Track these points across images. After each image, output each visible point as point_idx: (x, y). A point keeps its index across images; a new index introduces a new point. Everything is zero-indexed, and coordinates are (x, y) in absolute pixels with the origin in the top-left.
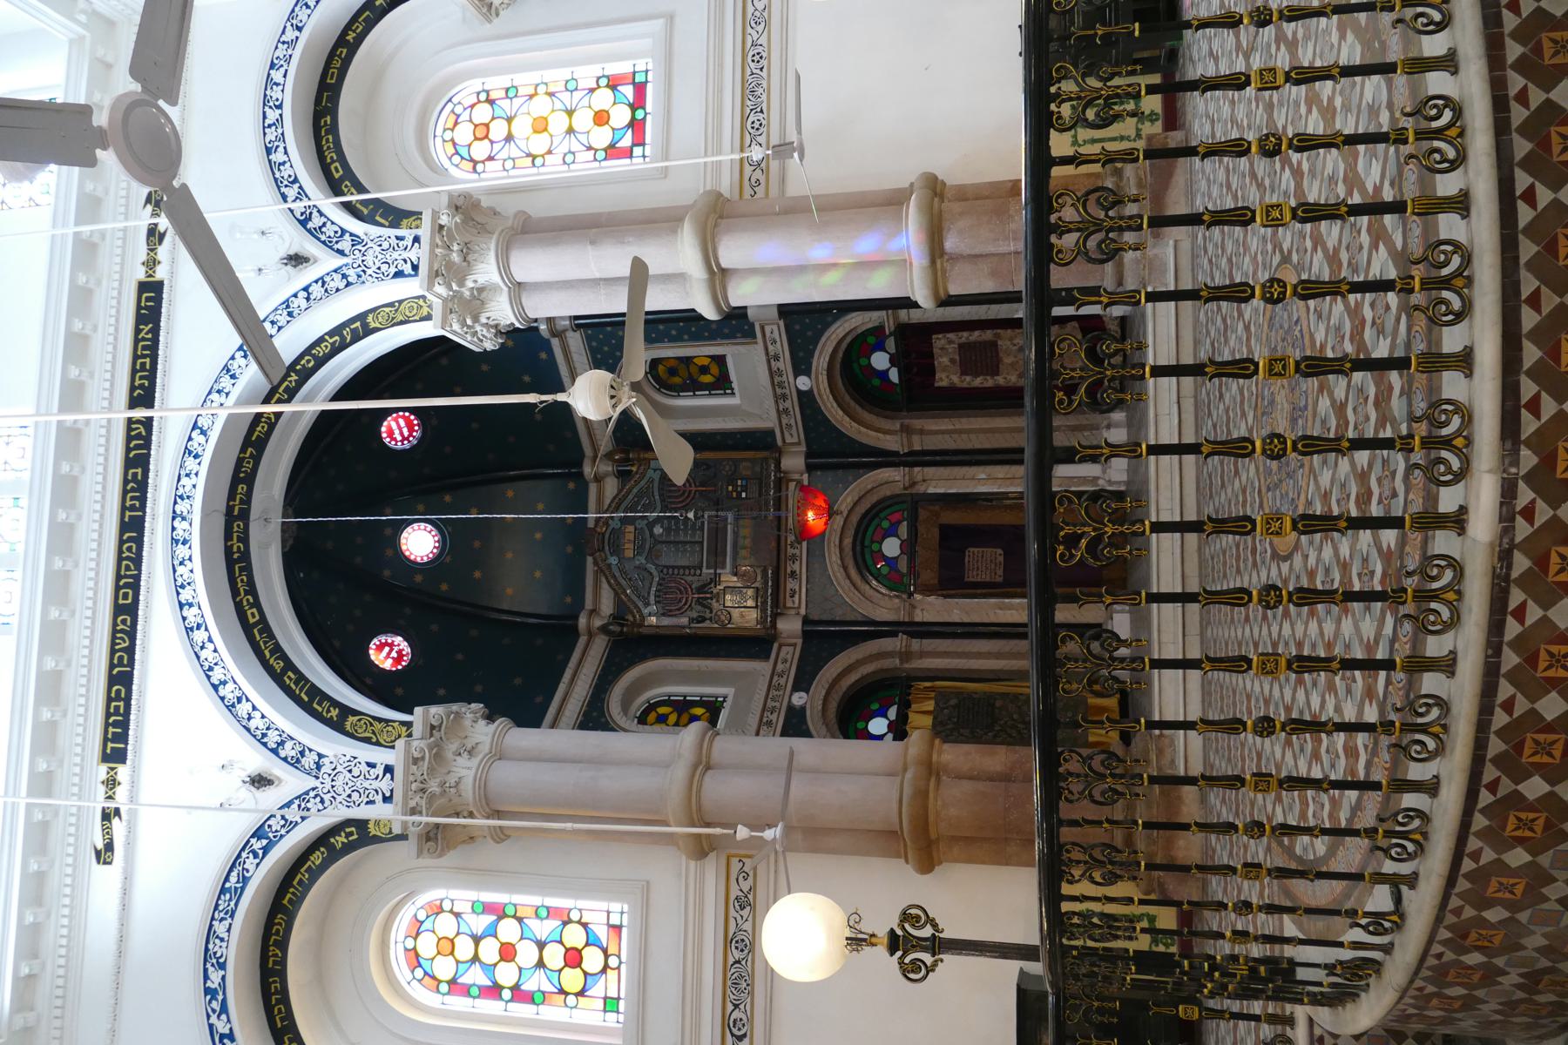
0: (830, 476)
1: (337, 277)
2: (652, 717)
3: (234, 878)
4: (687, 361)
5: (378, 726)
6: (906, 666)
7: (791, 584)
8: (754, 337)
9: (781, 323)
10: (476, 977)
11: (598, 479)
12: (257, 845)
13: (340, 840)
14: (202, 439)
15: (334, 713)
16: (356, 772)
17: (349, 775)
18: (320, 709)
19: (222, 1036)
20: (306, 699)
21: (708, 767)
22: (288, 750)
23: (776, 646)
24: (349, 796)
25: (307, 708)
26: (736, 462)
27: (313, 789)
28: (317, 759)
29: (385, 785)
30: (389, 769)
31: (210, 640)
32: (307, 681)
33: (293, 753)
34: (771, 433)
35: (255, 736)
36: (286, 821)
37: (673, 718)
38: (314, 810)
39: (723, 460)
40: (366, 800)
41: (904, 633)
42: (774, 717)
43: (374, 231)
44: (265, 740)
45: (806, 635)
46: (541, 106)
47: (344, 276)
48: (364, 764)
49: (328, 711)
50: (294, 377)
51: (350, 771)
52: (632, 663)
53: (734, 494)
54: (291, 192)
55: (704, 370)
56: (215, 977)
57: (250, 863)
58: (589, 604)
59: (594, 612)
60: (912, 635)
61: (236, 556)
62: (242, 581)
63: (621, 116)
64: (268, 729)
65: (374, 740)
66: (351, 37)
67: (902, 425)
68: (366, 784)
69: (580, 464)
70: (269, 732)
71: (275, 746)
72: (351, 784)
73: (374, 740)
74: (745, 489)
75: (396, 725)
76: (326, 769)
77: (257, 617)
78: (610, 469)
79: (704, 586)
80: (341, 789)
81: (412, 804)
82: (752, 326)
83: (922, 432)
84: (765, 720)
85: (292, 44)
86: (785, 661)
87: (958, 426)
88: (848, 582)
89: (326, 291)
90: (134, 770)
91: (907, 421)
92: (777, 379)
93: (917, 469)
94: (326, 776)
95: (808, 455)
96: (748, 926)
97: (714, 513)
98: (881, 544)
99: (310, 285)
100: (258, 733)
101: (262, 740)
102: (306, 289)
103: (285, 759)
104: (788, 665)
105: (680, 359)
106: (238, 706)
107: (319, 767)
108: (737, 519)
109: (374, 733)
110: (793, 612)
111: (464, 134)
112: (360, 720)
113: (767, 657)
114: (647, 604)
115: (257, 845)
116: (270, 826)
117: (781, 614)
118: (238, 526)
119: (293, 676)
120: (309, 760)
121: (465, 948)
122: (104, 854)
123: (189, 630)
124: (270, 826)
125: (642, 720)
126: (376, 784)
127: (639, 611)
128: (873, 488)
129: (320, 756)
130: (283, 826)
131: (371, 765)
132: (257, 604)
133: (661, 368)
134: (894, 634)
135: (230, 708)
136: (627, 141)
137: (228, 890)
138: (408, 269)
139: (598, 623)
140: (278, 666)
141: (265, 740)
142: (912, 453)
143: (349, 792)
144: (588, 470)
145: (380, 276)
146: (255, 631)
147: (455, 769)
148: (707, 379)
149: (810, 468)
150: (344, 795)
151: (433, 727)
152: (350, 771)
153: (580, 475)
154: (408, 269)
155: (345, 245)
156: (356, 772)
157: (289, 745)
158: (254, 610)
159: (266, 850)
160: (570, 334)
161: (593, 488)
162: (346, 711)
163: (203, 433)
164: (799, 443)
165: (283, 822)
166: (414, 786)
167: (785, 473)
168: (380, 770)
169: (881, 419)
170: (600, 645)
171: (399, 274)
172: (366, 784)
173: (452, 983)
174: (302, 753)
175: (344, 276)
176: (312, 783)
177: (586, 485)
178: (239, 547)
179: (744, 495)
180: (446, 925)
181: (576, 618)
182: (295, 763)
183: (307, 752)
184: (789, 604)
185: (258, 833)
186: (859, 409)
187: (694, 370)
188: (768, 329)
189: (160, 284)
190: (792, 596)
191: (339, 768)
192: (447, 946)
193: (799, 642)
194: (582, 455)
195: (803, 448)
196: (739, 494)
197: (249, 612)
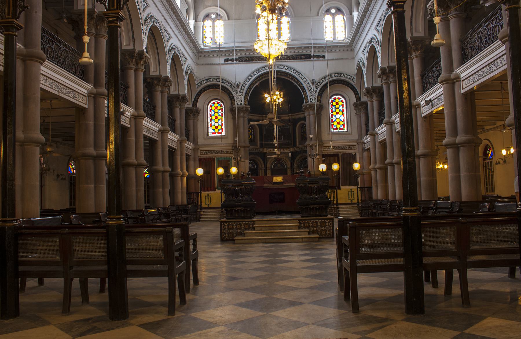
2: (249, 129)
3: (224, 81)
11: (288, 116)
13: (231, 95)
14: (286, 68)
29: (239, 104)
30: (241, 104)
37: (249, 133)
43: (317, 94)
45: (264, 153)
47: (310, 90)
50: (296, 81)
54: (323, 80)
57: (227, 84)
60: (265, 170)
63: (338, 126)
66: (349, 85)
69: (291, 113)
85: (347, 78)
90: (238, 63)
96: (224, 153)
101: (244, 83)
102: (309, 83)
107: (241, 93)
111: (337, 100)
120: (241, 91)
122: (226, 60)
125: (249, 128)
131: (242, 101)
134: (265, 167)
135: (248, 78)
136: (334, 127)
137: (224, 81)
138: (311, 100)
144: (290, 114)
153: (289, 113)
154: (311, 100)
155: (315, 90)
161: (287, 115)
162: (248, 94)
163: (287, 69)
168: (241, 103)
171: (311, 99)
173: (211, 109)
175: (310, 90)
189: (311, 59)
192: (216, 108)
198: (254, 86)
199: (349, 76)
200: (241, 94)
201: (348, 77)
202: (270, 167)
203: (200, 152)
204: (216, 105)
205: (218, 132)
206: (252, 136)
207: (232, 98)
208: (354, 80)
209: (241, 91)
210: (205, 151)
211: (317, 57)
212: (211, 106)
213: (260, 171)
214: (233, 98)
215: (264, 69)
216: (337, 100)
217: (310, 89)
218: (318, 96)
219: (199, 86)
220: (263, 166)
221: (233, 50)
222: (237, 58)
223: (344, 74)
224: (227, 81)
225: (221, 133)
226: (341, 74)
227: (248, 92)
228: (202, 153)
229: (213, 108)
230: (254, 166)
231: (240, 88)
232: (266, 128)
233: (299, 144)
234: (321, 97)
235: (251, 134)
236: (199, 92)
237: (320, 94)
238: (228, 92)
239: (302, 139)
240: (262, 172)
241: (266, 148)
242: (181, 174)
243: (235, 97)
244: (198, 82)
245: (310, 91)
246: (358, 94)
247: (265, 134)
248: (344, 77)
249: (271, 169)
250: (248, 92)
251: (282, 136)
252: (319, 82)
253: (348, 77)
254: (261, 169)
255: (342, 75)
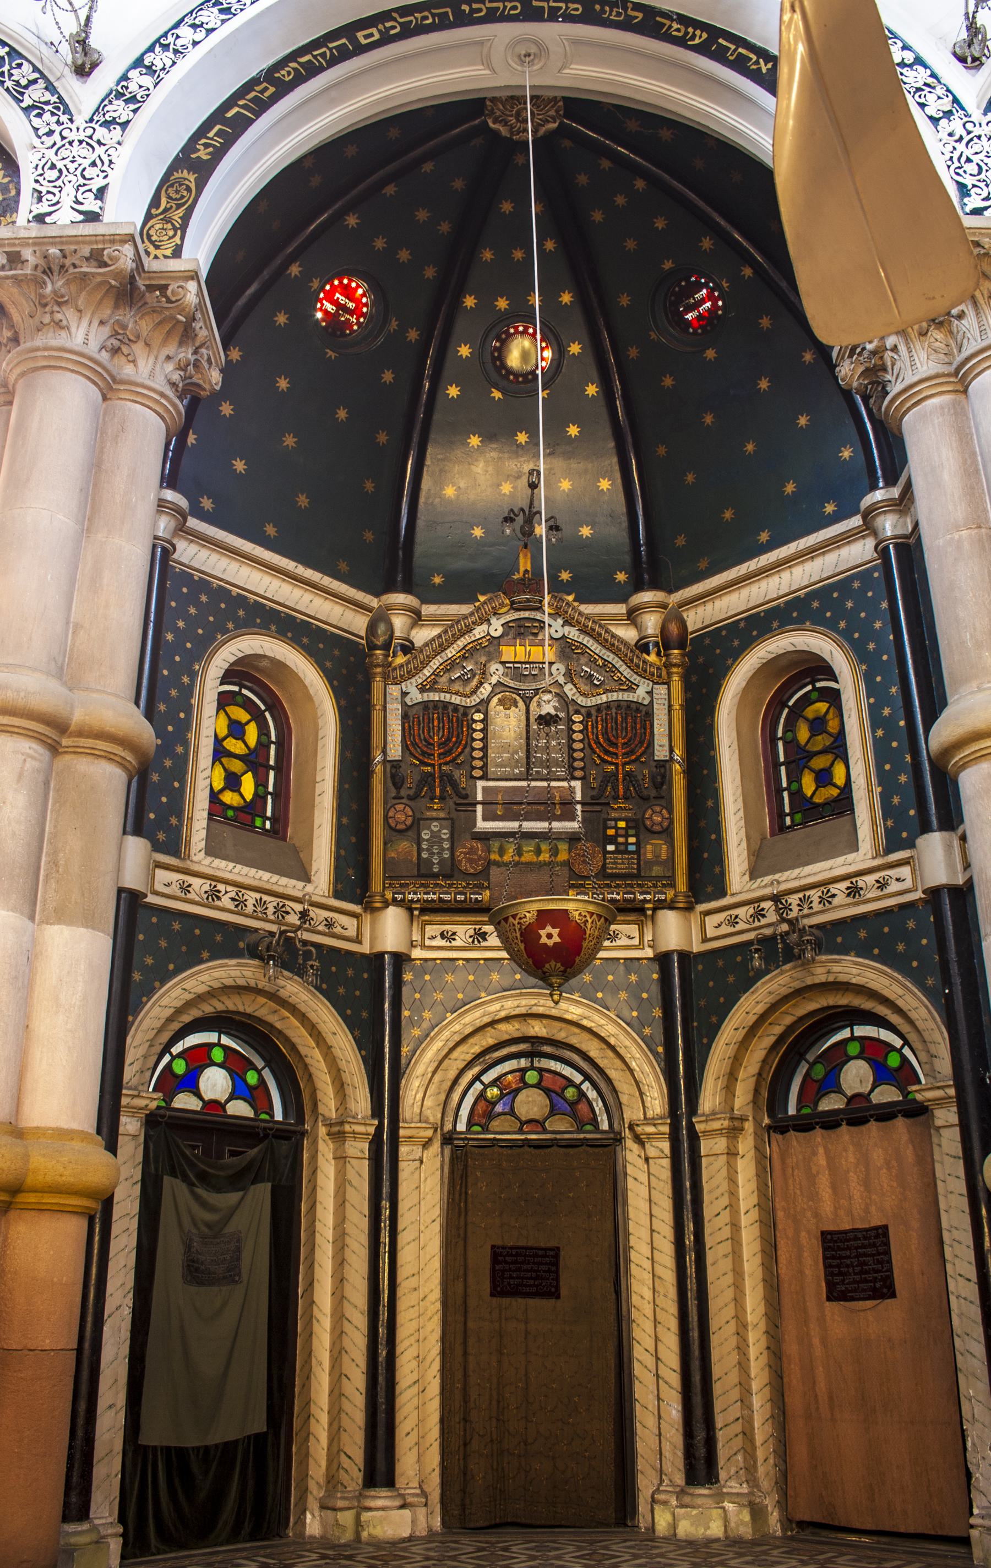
0: (651, 993)
1: (946, 104)
2: (241, 715)
4: (839, 749)
5: (177, 215)
6: (322, 1131)
7: (463, 932)
8: (888, 851)
9: (918, 895)
11: (632, 616)
15: (203, 154)
16: (90, 172)
17: (86, 163)
18: (211, 135)
20: (229, 115)
21: (54, 749)
22: (138, 79)
23: (357, 909)
24: (53, 167)
25: (217, 116)
26: (667, 832)
27: (71, 120)
28: (123, 120)
32: (258, 115)
33: (133, 87)
34: (721, 891)
35: (165, 35)
36: (26, 87)
38: (37, 122)
39: (670, 811)
40: (44, 190)
41: (379, 1129)
42: (226, 902)
44: (158, 49)
48: (103, 183)
49: (206, 146)
51: (94, 164)
52: (330, 676)
53: (611, 832)
55: (824, 778)
58: (427, 610)
59: (417, 618)
60: (376, 1142)
61: (466, 8)
62: (426, 18)
64: (176, 52)
65: (154, 211)
67: (743, 1119)
68: (69, 190)
70: (170, 54)
71: (147, 63)
72: (72, 167)
73: (154, 211)
74: (622, 850)
75: (177, 240)
76: (101, 133)
77: (364, 42)
78: (650, 631)
79: (454, 785)
80: (63, 153)
81: (27, 254)
82: (911, 845)
83: (732, 1154)
84: (221, 887)
86: (330, 924)
87: (744, 1221)
88: (469, 1030)
89: (918, 90)
91: (749, 1126)
92: (815, 894)
93: (666, 1146)
94: (89, 132)
95: (684, 956)
97: (578, 797)
98: (538, 1086)
99: (926, 66)
100: (170, 39)
101: (160, 43)
103: (125, 77)
104: (321, 928)
105: (841, 735)
106: (215, 10)
107: (106, 124)
108: (573, 838)
109: (166, 210)
110: (416, 937)
112: (188, 189)
113: (337, 895)
114: (422, 689)
116: (20, 66)
117: (412, 915)
118: (515, 8)
119: (267, 94)
124: (20, 66)
126: (67, 198)
127: (411, 675)
128: (631, 1071)
129: (124, 125)
130: (18, 83)
131: (101, 193)
132: (386, 39)
133: (822, 707)
134: (377, 1111)
139: (399, 623)
140: (285, 74)
141: (158, 49)
142: (694, 1138)
143: (60, 165)
144: (647, 596)
146: (344, 41)
147: (85, 323)
148: (808, 784)
149: (663, 959)
150: (54, 159)
151: (164, 288)
152: (94, 164)
153: (638, 586)
156: (90, 172)
157: (147, 81)
158: (377, 36)
160: (870, 543)
161: (621, 609)
164: (705, 940)
165: (24, 82)
166: (54, 251)
167: (653, 918)
168: (91, 204)
169: (751, 1083)
170: (358, 623)
172: (69, 190)
174: (133, 99)
175: (948, 114)
177: (624, 600)
178: (480, 10)
179: (611, 848)
181: (408, 590)
183: (132, 107)
184: (431, 930)
186: (768, 1041)
187: (820, 762)
188: (905, 871)
190: (443, 936)
191: (100, 150)
193: (365, 949)
194: (670, 592)
195: (697, 947)
196: (612, 840)
197: (374, 31)
198: (275, 99)
202: (434, 1115)
206: (260, 783)
213: (326, 1149)
220: (361, 1101)
230: (256, 1095)
231: (104, 79)
232: (415, 696)
233: (754, 873)
235: (255, 761)
239: (779, 828)
240: (341, 1159)
241: (408, 907)
247: (395, 751)
249: (448, 1139)
251: (577, 784)
254: (338, 1136)
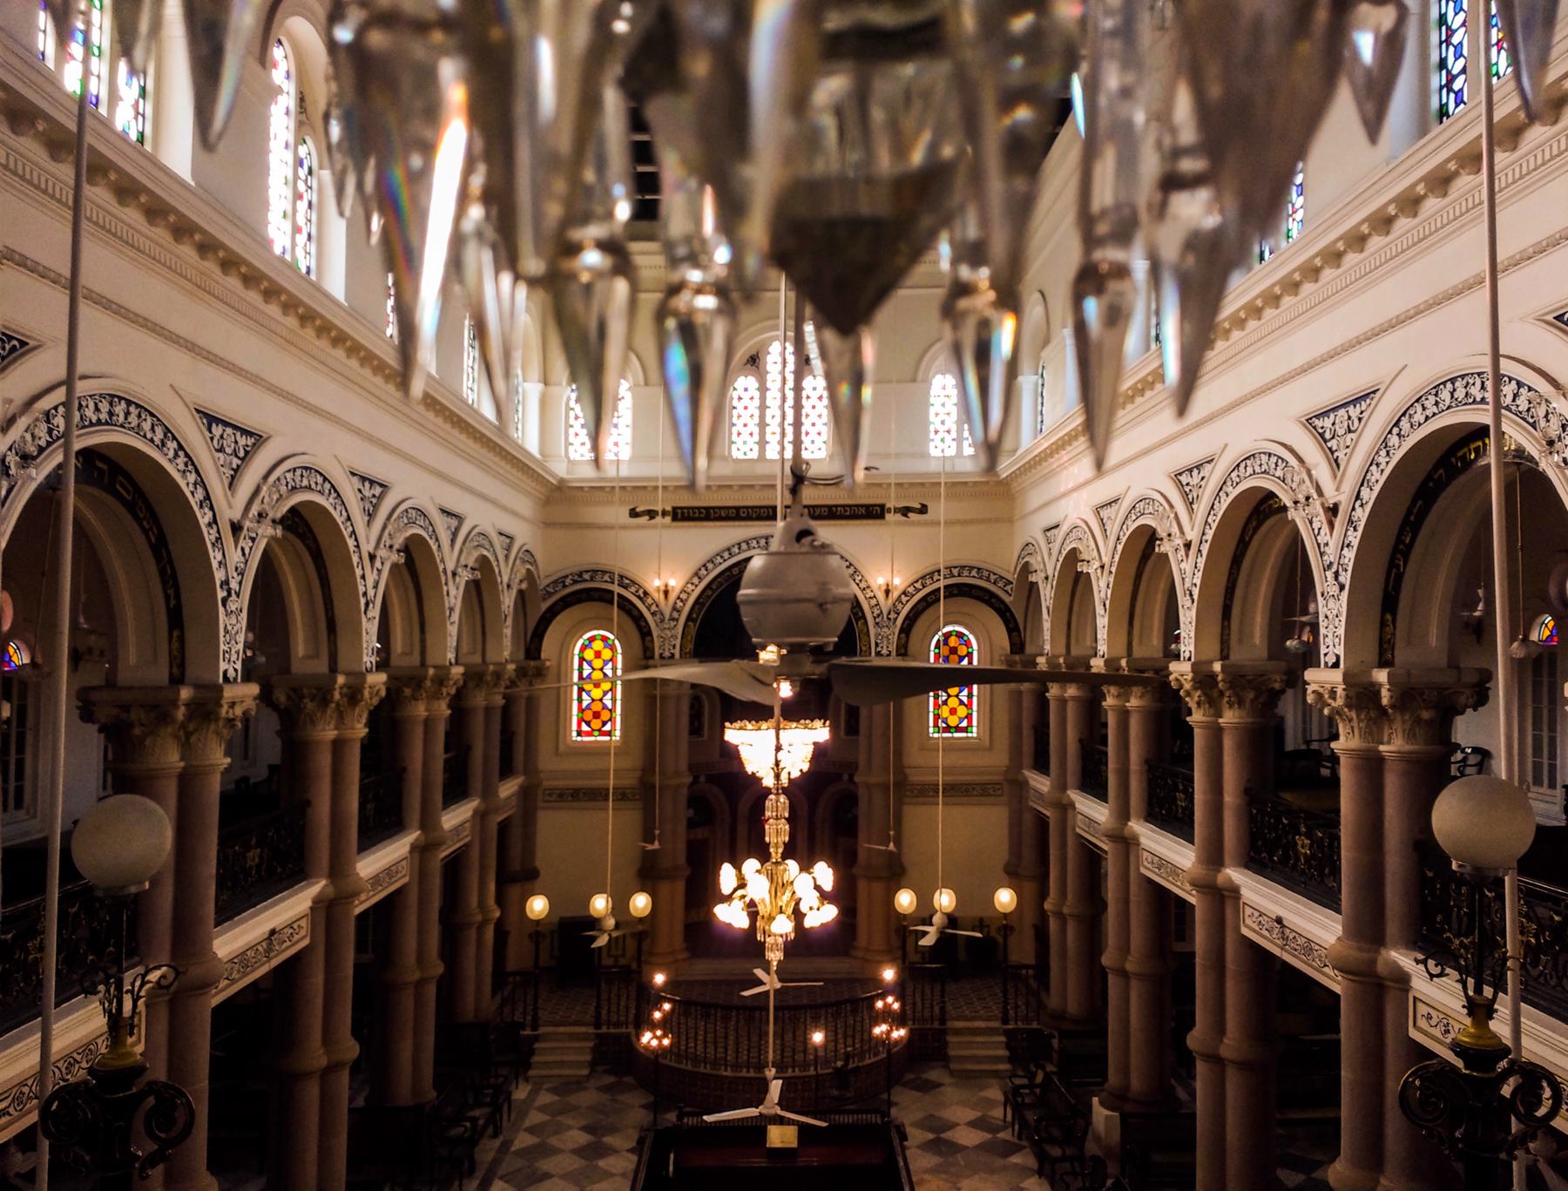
3: (627, 581)
10: (587, 671)
12: (641, 593)
13: (643, 624)
19: (564, 582)
29: (667, 654)
30: (673, 655)
31: (725, 561)
46: (945, 712)
47: (879, 615)
54: (918, 585)
56: (586, 576)
57: (633, 589)
115: (641, 593)
120: (675, 615)
121: (598, 663)
123: (729, 549)
131: (674, 647)
138: (879, 649)
145: (877, 635)
154: (879, 649)
159: (639, 597)
171: (877, 645)
176: (667, 617)
180: (607, 654)
182: (674, 608)
185: (646, 593)
192: (598, 654)
199: (994, 574)
200: (673, 624)
201: (993, 577)
203: (544, 794)
204: (598, 645)
205: (599, 730)
207: (645, 633)
208: (1008, 588)
209: (675, 615)
210: (557, 792)
211: (905, 511)
212: (583, 648)
214: (649, 633)
215: (744, 546)
216: (953, 641)
217: (877, 612)
218: (900, 633)
219: (550, 594)
221: (656, 488)
222: (669, 508)
223: (979, 569)
224: (634, 582)
225: (609, 733)
226: (972, 568)
227: (694, 616)
228: (547, 798)
229: (589, 654)
234: (908, 636)
236: (550, 609)
237: (906, 630)
238: (635, 613)
242: (479, 918)
243: (655, 634)
244: (547, 581)
245: (877, 620)
246: (1019, 631)
248: (981, 578)
250: (694, 616)
252: (904, 593)
253: (993, 577)
255: (974, 573)
